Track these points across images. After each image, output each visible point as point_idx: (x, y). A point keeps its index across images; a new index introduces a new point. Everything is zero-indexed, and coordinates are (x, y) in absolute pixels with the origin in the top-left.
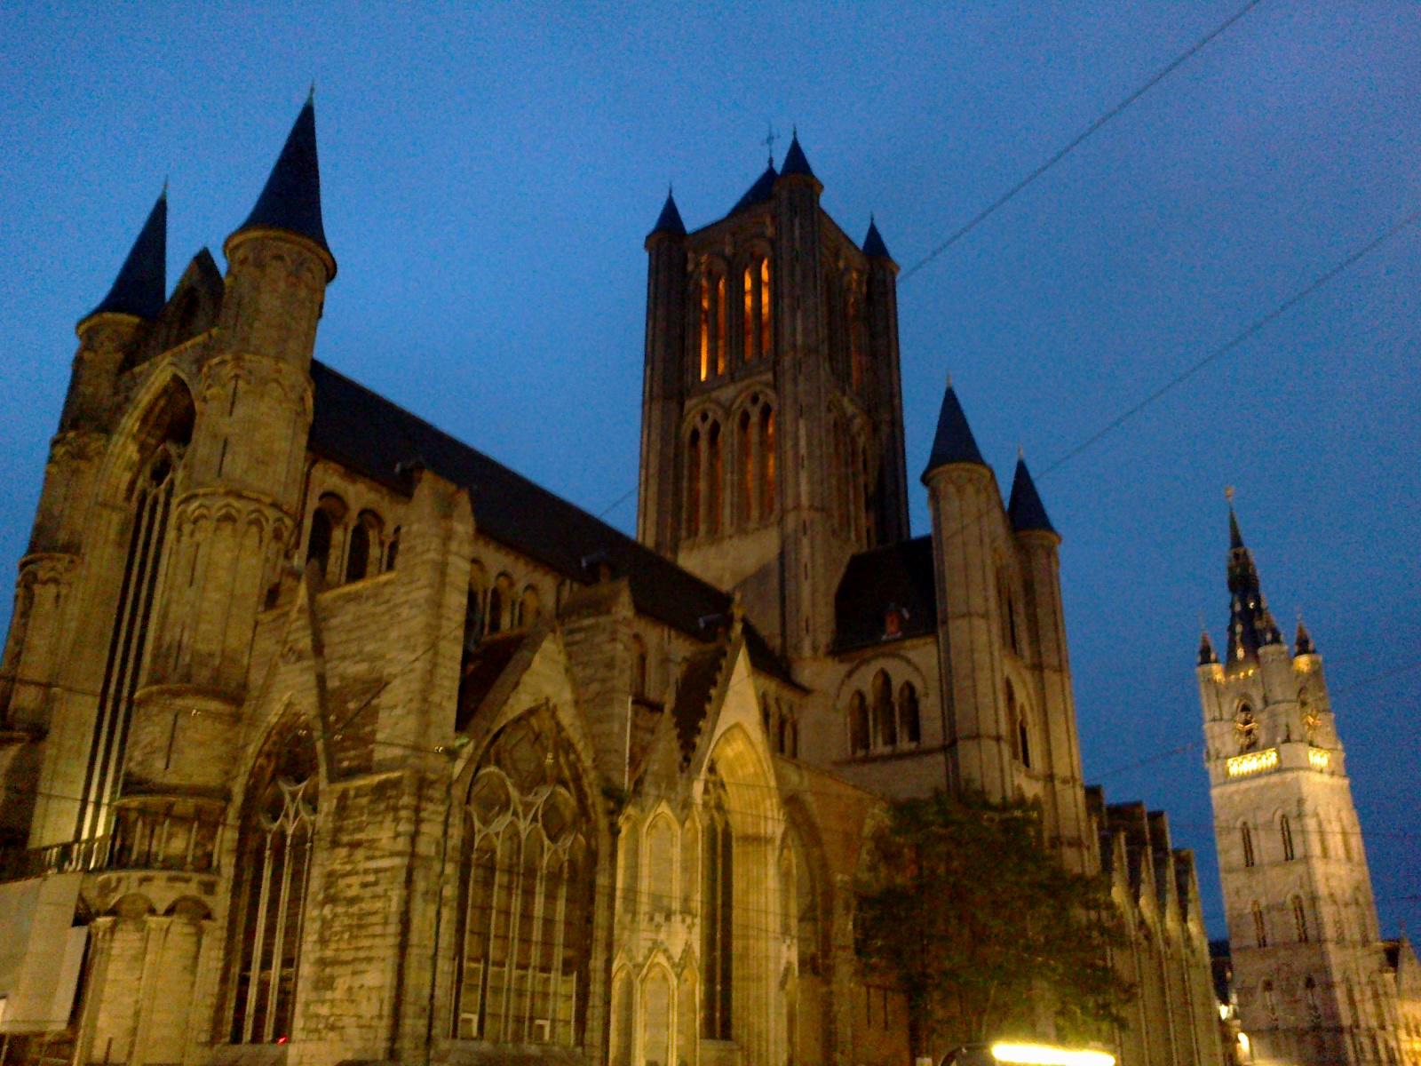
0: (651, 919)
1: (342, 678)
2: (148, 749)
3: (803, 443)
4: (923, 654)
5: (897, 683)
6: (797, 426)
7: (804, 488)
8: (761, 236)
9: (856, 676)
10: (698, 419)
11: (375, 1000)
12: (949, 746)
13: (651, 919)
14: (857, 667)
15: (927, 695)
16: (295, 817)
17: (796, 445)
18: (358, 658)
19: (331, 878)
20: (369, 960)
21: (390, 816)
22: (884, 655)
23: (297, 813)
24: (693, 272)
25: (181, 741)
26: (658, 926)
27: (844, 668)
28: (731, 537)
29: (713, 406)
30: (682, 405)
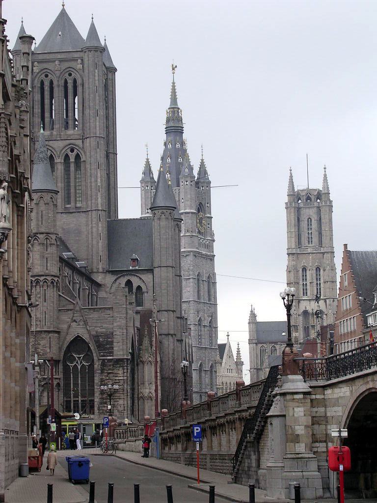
1: (97, 332)
3: (99, 180)
4: (148, 278)
5: (135, 286)
7: (99, 200)
11: (122, 406)
16: (80, 364)
19: (102, 380)
20: (120, 399)
21: (121, 369)
22: (130, 275)
25: (52, 345)
27: (115, 277)
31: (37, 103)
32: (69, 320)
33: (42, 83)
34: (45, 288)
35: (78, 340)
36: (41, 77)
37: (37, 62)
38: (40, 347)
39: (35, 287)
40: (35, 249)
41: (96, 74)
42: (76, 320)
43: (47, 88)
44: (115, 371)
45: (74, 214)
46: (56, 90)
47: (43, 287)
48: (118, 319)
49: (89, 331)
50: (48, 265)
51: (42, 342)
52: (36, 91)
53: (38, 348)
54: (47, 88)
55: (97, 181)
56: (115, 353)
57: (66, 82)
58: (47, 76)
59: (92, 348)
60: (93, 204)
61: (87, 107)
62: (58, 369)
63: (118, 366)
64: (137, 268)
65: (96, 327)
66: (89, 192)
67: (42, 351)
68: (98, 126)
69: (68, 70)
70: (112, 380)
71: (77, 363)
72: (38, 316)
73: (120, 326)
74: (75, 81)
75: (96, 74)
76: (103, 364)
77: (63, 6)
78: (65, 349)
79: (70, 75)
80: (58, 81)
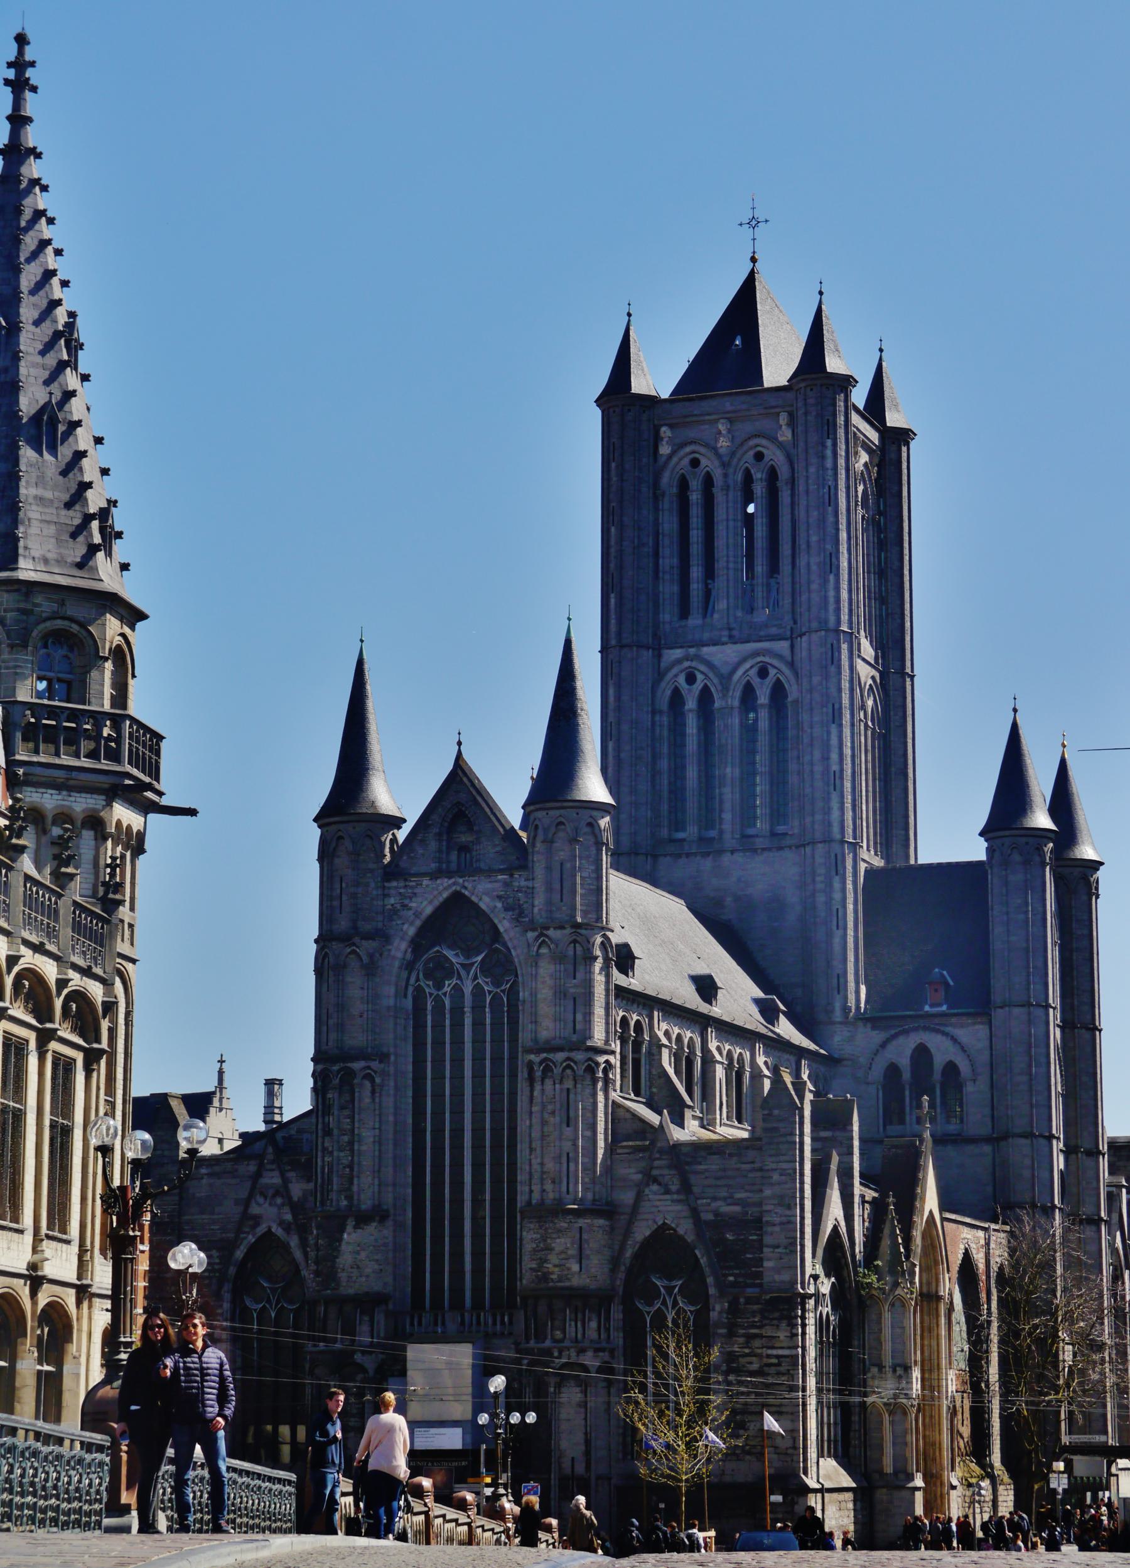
0: (894, 1371)
1: (717, 1214)
2: (563, 1256)
4: (974, 1035)
5: (939, 1062)
6: (829, 733)
8: (773, 439)
9: (892, 1047)
10: (682, 679)
12: (998, 1138)
13: (894, 1371)
14: (894, 1037)
15: (974, 1081)
16: (673, 1308)
17: (826, 758)
18: (729, 1201)
21: (784, 1324)
22: (926, 1029)
23: (675, 1303)
24: (670, 457)
26: (900, 1377)
27: (878, 1037)
28: (732, 852)
29: (703, 668)
30: (660, 656)
31: (667, 541)
32: (640, 1176)
33: (683, 485)
34: (569, 1084)
35: (662, 1235)
36: (679, 467)
37: (671, 426)
38: (554, 1259)
39: (542, 1084)
40: (541, 971)
41: (829, 452)
42: (660, 1179)
43: (695, 497)
44: (768, 1331)
45: (766, 854)
46: (719, 497)
47: (561, 1082)
48: (776, 1177)
49: (695, 1213)
50: (579, 1017)
51: (560, 1243)
52: (666, 506)
53: (546, 1261)
54: (695, 497)
55: (828, 758)
56: (767, 1279)
57: (748, 478)
58: (695, 463)
59: (703, 1261)
60: (816, 827)
61: (804, 546)
62: (608, 1319)
63: (776, 1315)
64: (944, 1008)
65: (715, 1199)
66: (808, 791)
67: (556, 1269)
68: (832, 600)
69: (752, 443)
70: (760, 1356)
71: (664, 1303)
72: (550, 1165)
73: (782, 1197)
74: (773, 475)
75: (829, 452)
76: (734, 1310)
77: (754, 260)
78: (628, 1262)
79: (759, 457)
80: (726, 475)
